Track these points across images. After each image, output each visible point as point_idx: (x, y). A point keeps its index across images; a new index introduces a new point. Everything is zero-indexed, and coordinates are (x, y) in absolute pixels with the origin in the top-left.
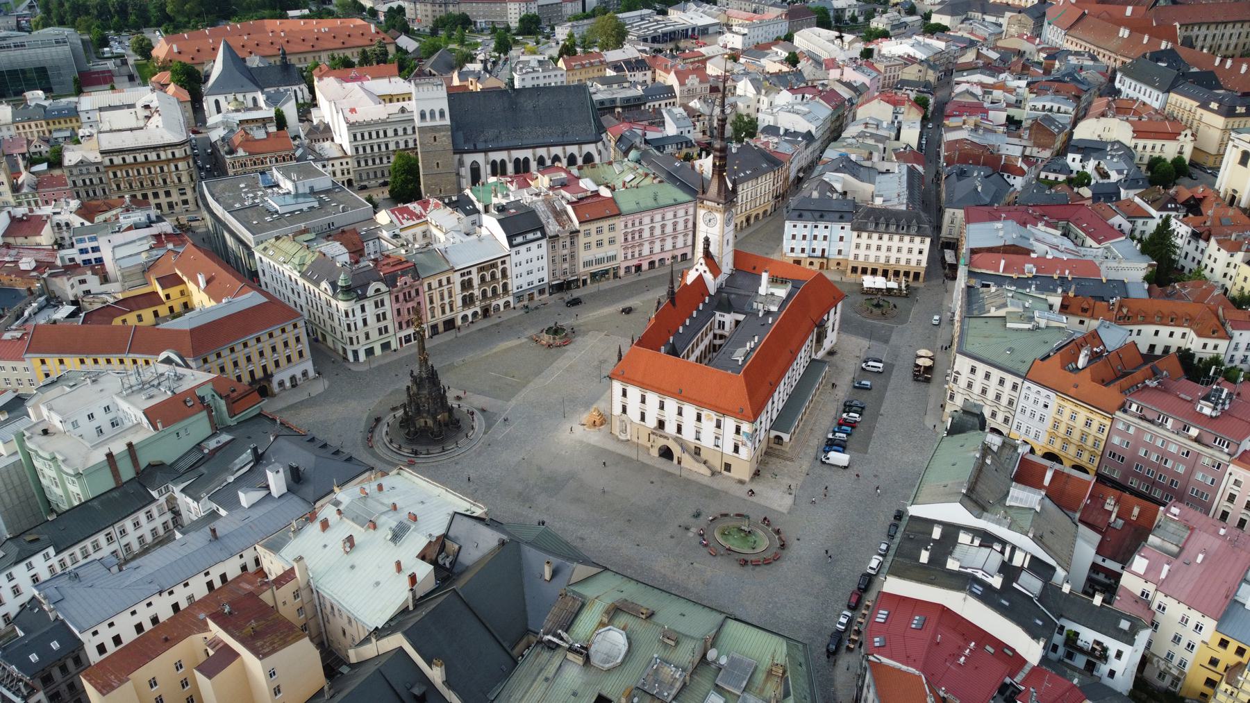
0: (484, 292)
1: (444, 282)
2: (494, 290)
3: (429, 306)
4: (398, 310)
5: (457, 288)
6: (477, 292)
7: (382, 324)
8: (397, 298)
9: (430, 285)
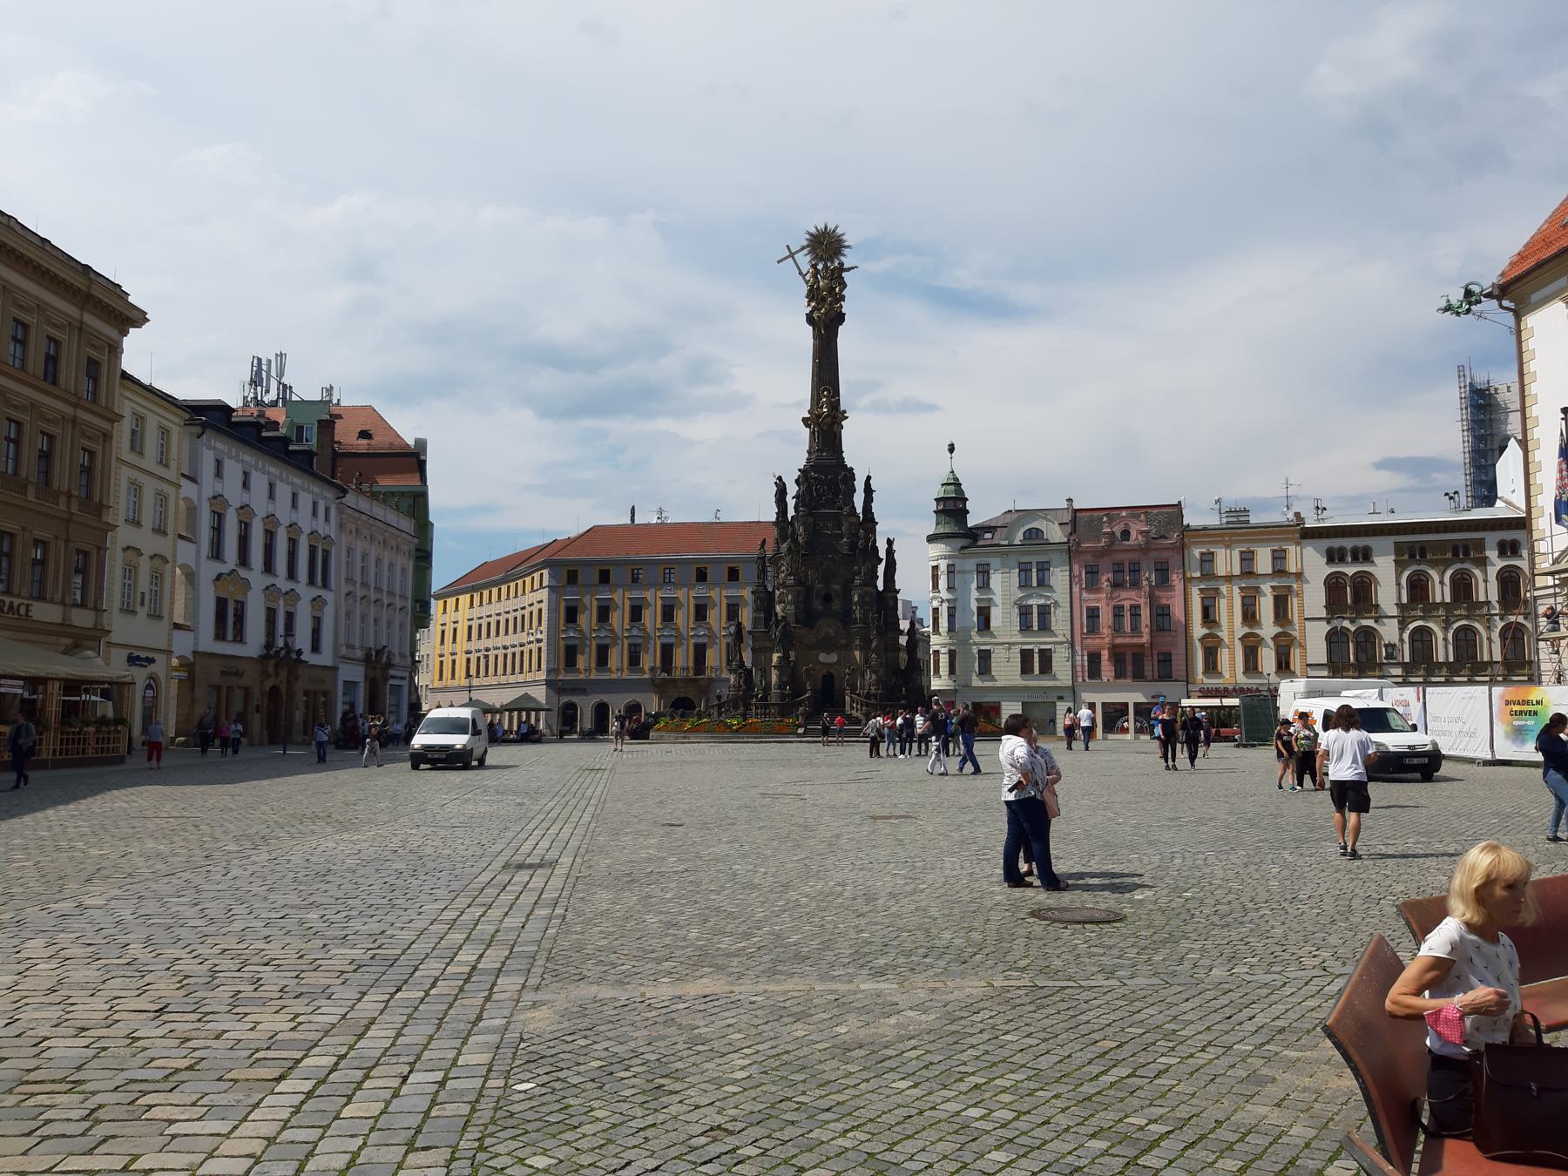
0: (1422, 639)
1: (1263, 562)
2: (1465, 642)
3: (1198, 631)
4: (1093, 614)
5: (1313, 598)
6: (1389, 631)
7: (1036, 642)
8: (1093, 572)
9: (1208, 559)
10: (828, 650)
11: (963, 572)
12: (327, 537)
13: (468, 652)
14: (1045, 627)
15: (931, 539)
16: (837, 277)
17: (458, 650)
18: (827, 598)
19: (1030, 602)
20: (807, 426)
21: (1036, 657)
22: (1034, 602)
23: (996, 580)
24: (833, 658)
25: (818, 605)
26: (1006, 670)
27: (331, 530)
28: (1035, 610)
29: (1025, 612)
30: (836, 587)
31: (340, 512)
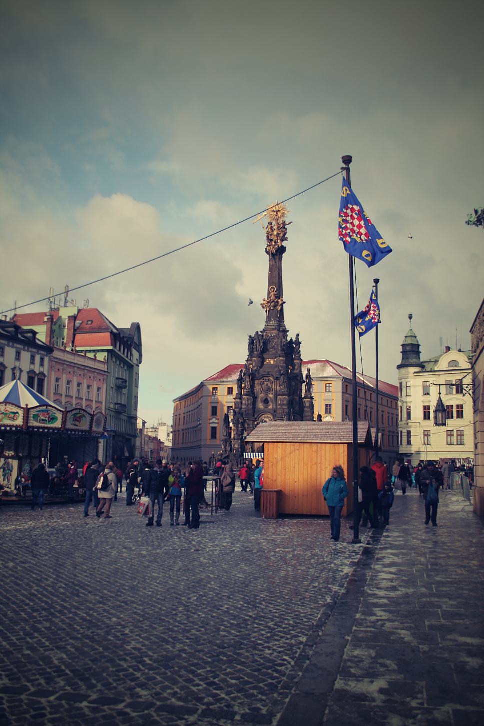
11: (415, 386)
12: (42, 374)
13: (183, 430)
15: (399, 367)
16: (283, 228)
17: (180, 430)
18: (266, 401)
20: (264, 308)
21: (455, 434)
25: (261, 406)
27: (45, 370)
28: (455, 408)
30: (271, 396)
31: (51, 361)
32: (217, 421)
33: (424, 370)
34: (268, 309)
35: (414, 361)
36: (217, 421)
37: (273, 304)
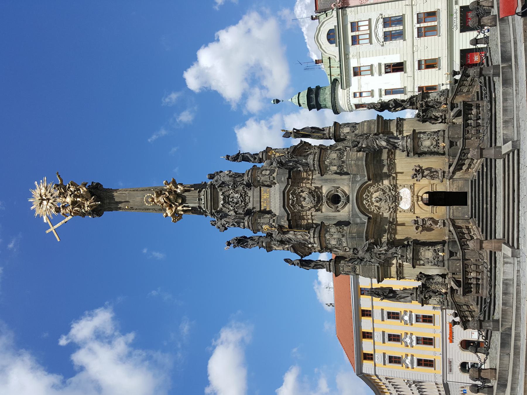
7: (411, 26)
10: (396, 199)
11: (360, 86)
14: (400, 20)
19: (381, 35)
22: (381, 30)
23: (364, 62)
24: (405, 193)
26: (434, 47)
28: (387, 29)
29: (388, 37)
32: (409, 357)
33: (339, 77)
34: (180, 208)
35: (328, 91)
36: (409, 357)
37: (171, 197)
